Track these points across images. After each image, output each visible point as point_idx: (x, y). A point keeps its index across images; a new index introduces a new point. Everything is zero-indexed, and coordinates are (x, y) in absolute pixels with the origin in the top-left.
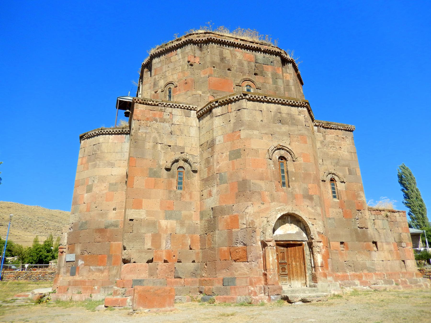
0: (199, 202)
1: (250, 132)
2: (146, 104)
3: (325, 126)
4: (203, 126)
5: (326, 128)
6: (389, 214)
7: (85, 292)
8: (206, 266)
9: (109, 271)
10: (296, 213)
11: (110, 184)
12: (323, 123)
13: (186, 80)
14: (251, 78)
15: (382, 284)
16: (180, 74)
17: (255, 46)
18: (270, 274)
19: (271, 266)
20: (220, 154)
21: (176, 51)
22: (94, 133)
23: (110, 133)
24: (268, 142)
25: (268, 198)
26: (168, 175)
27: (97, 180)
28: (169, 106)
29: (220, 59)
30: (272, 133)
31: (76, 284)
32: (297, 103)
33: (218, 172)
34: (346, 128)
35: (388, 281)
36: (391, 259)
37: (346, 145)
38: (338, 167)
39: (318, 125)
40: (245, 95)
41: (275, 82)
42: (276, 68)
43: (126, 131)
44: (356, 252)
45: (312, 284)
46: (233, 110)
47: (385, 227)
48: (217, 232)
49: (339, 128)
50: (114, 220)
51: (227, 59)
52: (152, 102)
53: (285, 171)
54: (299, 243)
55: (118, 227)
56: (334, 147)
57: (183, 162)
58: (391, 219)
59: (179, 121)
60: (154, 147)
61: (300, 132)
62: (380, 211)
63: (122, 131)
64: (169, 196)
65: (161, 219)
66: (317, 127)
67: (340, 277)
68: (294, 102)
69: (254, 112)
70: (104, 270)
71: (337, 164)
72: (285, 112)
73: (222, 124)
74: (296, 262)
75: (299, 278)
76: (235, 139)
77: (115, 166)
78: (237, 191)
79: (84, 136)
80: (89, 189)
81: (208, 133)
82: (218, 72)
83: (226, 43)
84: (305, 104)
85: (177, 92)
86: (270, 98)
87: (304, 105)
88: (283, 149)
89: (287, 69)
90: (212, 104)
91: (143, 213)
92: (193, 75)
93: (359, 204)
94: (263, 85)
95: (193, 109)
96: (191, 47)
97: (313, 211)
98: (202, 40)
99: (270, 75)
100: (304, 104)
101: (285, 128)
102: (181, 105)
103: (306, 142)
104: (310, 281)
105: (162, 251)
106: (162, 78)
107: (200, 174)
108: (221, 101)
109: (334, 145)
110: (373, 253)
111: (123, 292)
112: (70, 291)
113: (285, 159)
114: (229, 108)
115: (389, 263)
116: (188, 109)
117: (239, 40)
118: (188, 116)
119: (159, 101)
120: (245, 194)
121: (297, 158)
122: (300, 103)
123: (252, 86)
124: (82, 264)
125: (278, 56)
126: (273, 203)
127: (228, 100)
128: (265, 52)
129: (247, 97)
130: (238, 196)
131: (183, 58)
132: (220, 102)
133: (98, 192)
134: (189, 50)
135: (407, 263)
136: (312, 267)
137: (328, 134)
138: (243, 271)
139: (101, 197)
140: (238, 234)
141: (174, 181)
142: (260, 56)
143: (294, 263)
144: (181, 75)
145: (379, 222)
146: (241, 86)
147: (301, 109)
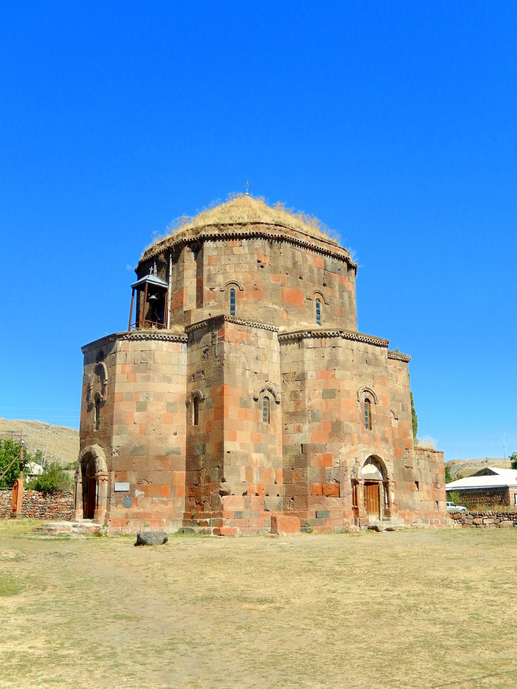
0: (281, 436)
2: (235, 323)
4: (287, 352)
6: (430, 454)
7: (153, 524)
8: (292, 500)
9: (174, 503)
11: (167, 403)
14: (321, 290)
15: (420, 523)
16: (246, 274)
17: (325, 247)
18: (361, 508)
19: (361, 502)
20: (312, 391)
22: (142, 336)
23: (164, 339)
26: (256, 405)
27: (153, 397)
28: (255, 326)
30: (360, 374)
31: (137, 516)
33: (310, 409)
35: (425, 520)
36: (428, 499)
38: (394, 402)
40: (341, 332)
41: (341, 296)
43: (183, 339)
44: (402, 491)
45: (386, 518)
46: (327, 346)
47: (426, 468)
48: (309, 468)
49: (398, 358)
50: (174, 446)
51: (299, 263)
53: (368, 413)
54: (376, 482)
55: (180, 455)
57: (268, 391)
58: (431, 459)
60: (244, 374)
63: (179, 338)
65: (252, 452)
68: (379, 342)
69: (347, 350)
70: (168, 501)
72: (371, 352)
73: (314, 358)
74: (373, 498)
75: (375, 513)
76: (329, 377)
77: (172, 381)
78: (330, 431)
79: (124, 336)
80: (142, 407)
81: (295, 363)
85: (243, 297)
88: (368, 391)
90: (303, 333)
91: (237, 446)
93: (408, 443)
94: (331, 299)
95: (275, 330)
96: (262, 242)
97: (388, 453)
98: (275, 236)
99: (337, 287)
101: (370, 369)
102: (265, 325)
104: (382, 515)
105: (254, 485)
106: (221, 272)
107: (282, 406)
108: (315, 333)
110: (415, 492)
111: (230, 522)
112: (132, 524)
113: (369, 401)
114: (323, 342)
115: (426, 503)
116: (270, 330)
117: (309, 237)
118: (271, 338)
119: (246, 320)
120: (339, 434)
123: (321, 300)
124: (141, 495)
126: (360, 445)
127: (323, 334)
128: (334, 256)
130: (331, 435)
131: (252, 254)
132: (313, 334)
133: (154, 412)
134: (259, 246)
136: (385, 503)
138: (335, 505)
139: (159, 418)
140: (331, 472)
141: (261, 412)
142: (329, 260)
143: (371, 500)
145: (422, 462)
146: (311, 300)
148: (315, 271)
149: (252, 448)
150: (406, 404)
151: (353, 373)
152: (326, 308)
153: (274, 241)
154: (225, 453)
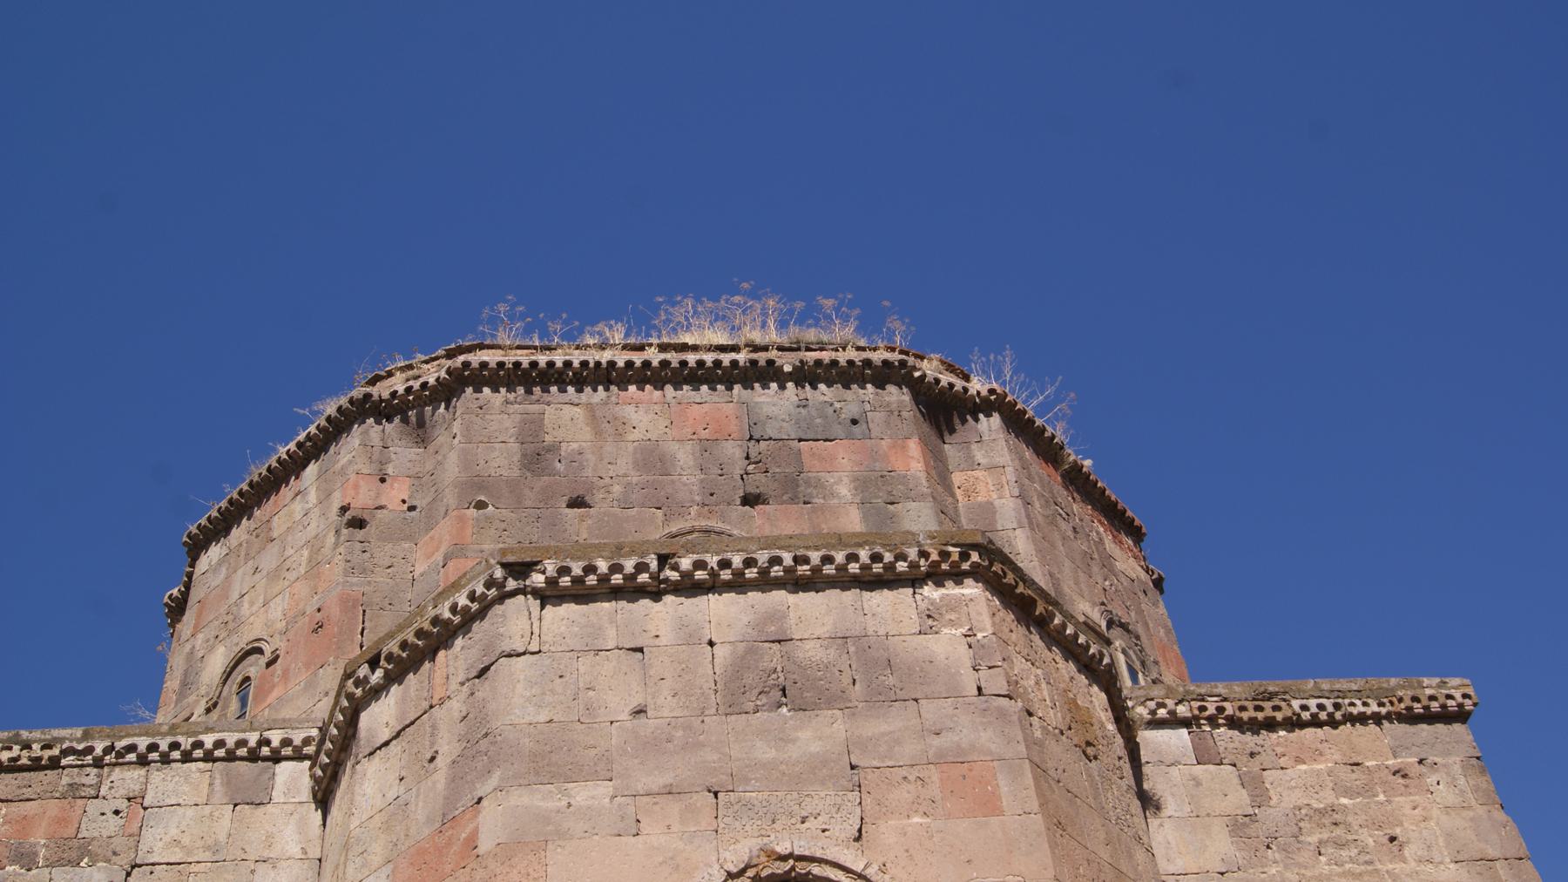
1: (542, 799)
3: (1245, 716)
5: (1255, 727)
12: (1225, 700)
13: (319, 610)
21: (297, 478)
24: (681, 845)
28: (132, 757)
29: (524, 455)
30: (713, 781)
32: (901, 557)
34: (1407, 702)
37: (1435, 812)
39: (1196, 718)
40: (520, 569)
42: (885, 448)
46: (454, 685)
49: (1355, 711)
56: (1341, 845)
59: (186, 840)
61: (936, 742)
66: (1184, 731)
69: (585, 663)
73: (391, 795)
76: (448, 868)
82: (503, 525)
83: (561, 373)
84: (965, 556)
86: (696, 557)
87: (955, 565)
89: (974, 447)
92: (364, 571)
99: (845, 491)
100: (955, 557)
102: (209, 740)
103: (989, 805)
108: (393, 647)
109: (1338, 831)
119: (61, 740)
122: (924, 554)
125: (891, 388)
127: (426, 626)
128: (806, 376)
129: (538, 579)
131: (325, 496)
132: (389, 658)
137: (1283, 762)
142: (776, 402)
144: (302, 589)
147: (942, 591)
148: (681, 455)
151: (640, 788)
153: (428, 409)
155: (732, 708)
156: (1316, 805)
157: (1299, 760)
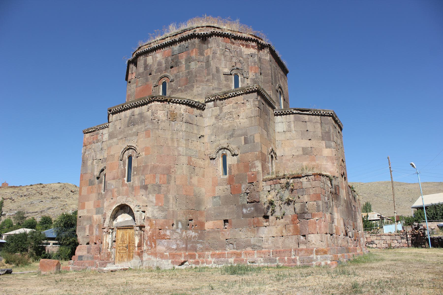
10: (126, 204)
12: (219, 96)
15: (262, 262)
25: (116, 194)
52: (92, 130)
62: (280, 179)
64: (98, 197)
65: (94, 215)
67: (216, 255)
71: (232, 136)
72: (137, 113)
84: (152, 99)
91: (85, 212)
99: (184, 63)
111: (72, 263)
119: (95, 128)
121: (139, 153)
128: (181, 40)
135: (309, 238)
149: (94, 211)
150: (251, 135)
152: (172, 85)
154: (78, 218)
155: (128, 126)
156: (229, 111)
157: (229, 104)
